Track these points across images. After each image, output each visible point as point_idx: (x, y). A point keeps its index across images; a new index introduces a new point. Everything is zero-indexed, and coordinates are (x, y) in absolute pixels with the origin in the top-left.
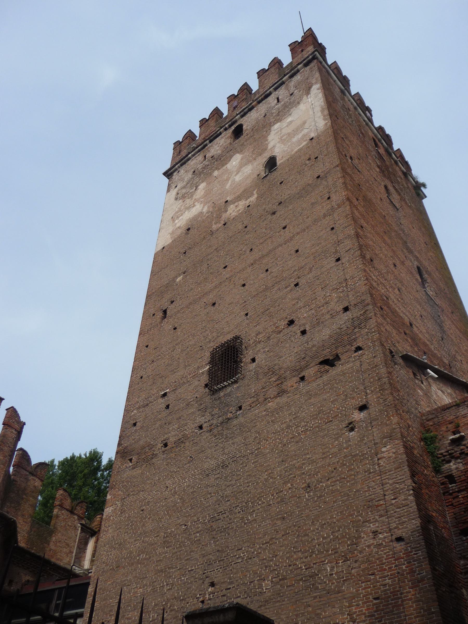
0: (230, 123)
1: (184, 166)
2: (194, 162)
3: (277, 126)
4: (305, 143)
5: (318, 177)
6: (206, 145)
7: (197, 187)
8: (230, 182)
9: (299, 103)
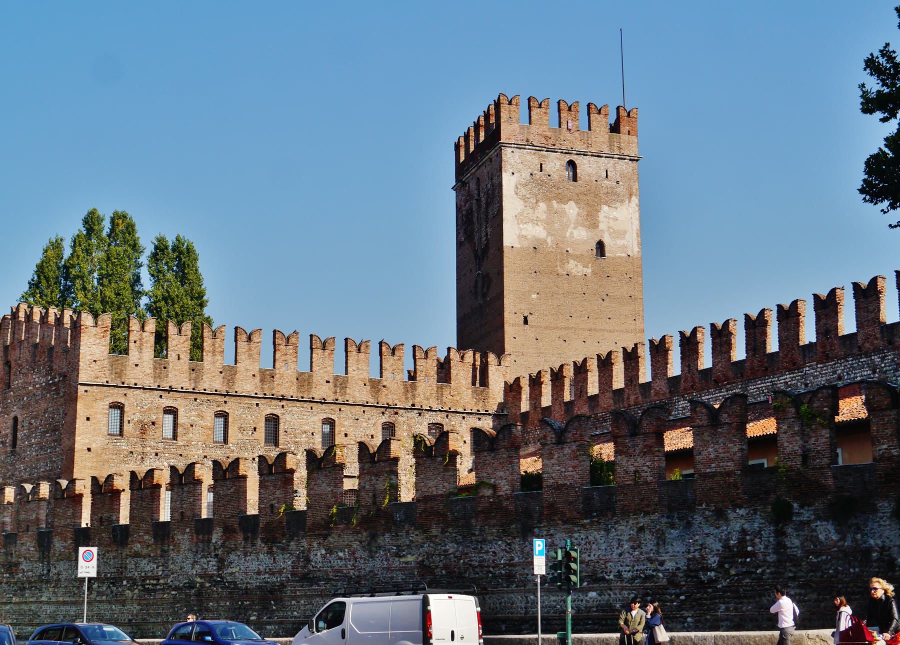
0: (567, 151)
2: (528, 158)
3: (605, 208)
4: (624, 255)
5: (631, 296)
6: (542, 151)
8: (569, 231)
9: (622, 201)
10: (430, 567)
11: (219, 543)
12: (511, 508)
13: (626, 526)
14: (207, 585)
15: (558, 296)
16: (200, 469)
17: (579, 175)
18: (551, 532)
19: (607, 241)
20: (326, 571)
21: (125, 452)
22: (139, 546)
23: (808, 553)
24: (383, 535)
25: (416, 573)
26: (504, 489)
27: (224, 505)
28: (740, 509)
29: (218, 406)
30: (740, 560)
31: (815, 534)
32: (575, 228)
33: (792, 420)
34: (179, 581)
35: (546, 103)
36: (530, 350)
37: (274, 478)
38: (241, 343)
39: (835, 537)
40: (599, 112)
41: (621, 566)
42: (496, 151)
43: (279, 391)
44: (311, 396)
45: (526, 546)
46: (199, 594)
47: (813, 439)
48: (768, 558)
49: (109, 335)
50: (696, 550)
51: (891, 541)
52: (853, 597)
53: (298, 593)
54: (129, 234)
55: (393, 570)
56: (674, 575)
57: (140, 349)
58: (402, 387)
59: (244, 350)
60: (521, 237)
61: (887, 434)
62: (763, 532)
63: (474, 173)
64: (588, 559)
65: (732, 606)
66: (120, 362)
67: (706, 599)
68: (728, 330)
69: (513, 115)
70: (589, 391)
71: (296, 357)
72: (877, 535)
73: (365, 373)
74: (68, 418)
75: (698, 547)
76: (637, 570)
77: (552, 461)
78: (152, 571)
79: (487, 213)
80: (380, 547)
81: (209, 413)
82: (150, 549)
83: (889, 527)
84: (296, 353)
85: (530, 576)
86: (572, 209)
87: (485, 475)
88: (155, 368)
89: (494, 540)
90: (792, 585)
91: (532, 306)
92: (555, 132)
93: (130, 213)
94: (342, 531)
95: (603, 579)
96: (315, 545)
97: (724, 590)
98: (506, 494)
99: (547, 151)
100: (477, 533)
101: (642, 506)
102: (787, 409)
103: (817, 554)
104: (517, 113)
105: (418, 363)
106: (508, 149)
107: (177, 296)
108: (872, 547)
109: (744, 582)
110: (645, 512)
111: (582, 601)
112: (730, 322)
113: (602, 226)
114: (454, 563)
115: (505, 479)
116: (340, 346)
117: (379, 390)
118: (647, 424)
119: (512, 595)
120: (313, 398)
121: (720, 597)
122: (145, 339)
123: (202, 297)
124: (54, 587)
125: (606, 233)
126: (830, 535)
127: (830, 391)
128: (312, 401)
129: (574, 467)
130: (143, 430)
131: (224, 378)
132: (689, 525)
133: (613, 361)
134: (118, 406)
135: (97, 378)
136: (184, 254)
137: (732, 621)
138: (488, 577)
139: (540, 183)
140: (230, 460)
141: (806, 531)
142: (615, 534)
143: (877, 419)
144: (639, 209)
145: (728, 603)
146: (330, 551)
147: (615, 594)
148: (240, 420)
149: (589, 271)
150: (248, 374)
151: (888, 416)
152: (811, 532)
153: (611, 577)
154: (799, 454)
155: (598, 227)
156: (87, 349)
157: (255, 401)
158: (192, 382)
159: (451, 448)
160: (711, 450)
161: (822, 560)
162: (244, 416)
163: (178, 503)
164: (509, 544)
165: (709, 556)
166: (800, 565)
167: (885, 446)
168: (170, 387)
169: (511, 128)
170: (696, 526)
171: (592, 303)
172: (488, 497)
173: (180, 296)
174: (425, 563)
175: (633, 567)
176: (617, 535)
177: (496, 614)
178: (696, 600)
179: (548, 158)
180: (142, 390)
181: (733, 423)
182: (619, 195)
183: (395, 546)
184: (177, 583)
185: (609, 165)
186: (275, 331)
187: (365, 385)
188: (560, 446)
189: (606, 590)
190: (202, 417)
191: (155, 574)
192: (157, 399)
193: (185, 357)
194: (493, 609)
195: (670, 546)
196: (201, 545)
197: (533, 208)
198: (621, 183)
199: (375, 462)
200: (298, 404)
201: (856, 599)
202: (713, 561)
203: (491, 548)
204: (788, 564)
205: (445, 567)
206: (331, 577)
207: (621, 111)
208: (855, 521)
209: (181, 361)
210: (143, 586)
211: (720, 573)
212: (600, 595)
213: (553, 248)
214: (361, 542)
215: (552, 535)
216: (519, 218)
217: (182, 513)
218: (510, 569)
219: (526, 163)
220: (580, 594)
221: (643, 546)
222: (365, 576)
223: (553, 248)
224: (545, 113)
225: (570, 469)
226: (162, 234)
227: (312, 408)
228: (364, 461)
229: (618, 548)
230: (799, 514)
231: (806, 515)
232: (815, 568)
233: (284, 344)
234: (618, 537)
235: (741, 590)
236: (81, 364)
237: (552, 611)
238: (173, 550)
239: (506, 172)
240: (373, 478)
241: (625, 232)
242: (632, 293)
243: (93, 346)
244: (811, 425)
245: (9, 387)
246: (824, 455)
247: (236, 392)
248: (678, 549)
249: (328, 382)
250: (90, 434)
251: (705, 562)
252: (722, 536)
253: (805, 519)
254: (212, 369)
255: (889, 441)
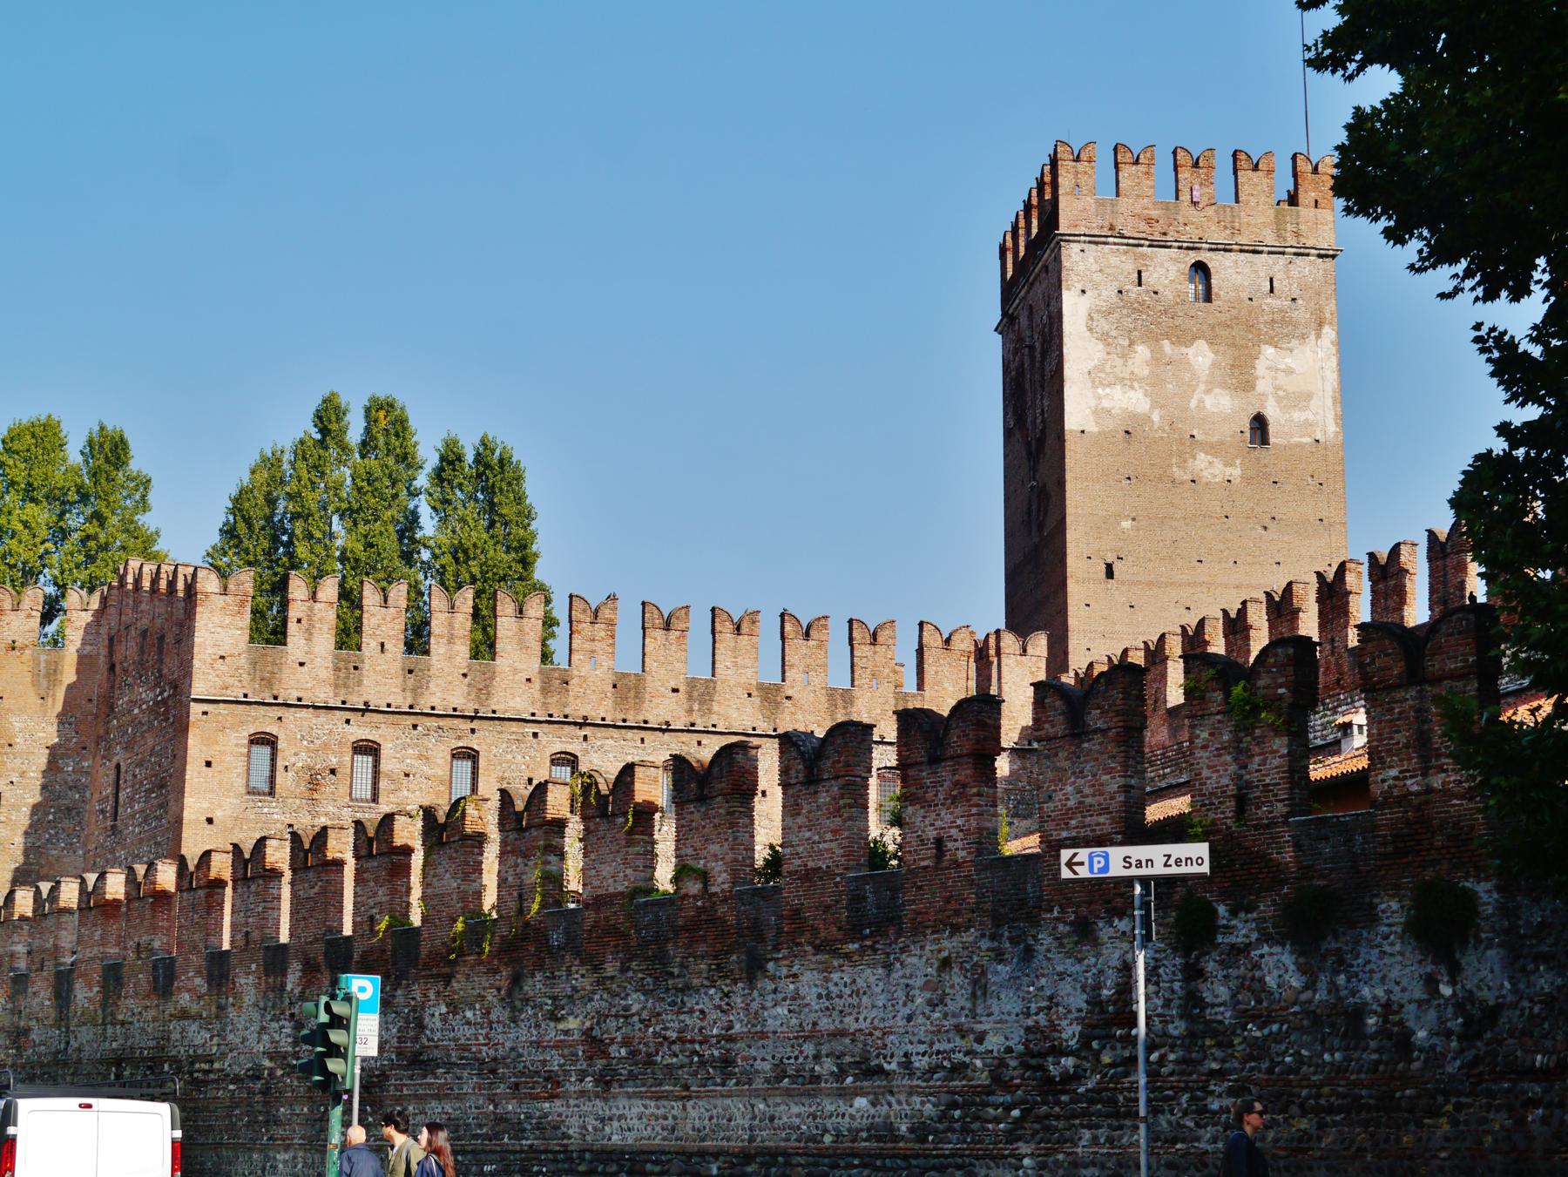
1: (1093, 246)
2: (1114, 260)
3: (1269, 351)
4: (1307, 440)
6: (1142, 246)
7: (1132, 343)
9: (1303, 337)
10: (602, 1041)
11: (296, 991)
12: (731, 919)
13: (921, 956)
14: (279, 1072)
15: (1175, 524)
16: (276, 849)
17: (1215, 290)
18: (795, 969)
19: (1271, 413)
20: (446, 1048)
21: (278, 825)
22: (187, 996)
23: (1245, 1016)
24: (533, 976)
25: (580, 1053)
26: (720, 880)
27: (304, 919)
28: (1120, 920)
29: (459, 738)
30: (1118, 1033)
31: (1258, 974)
32: (1208, 391)
33: (1219, 717)
34: (240, 1065)
35: (1148, 155)
36: (1118, 627)
37: (375, 864)
38: (504, 619)
39: (1296, 982)
40: (1256, 168)
41: (911, 1043)
42: (1052, 251)
43: (577, 710)
44: (641, 718)
45: (754, 1000)
46: (266, 1092)
47: (1257, 759)
48: (1170, 1026)
49: (248, 609)
50: (1040, 1009)
51: (1404, 990)
52: (1328, 1119)
53: (405, 1092)
54: (397, 435)
55: (545, 1047)
56: (1002, 1063)
57: (309, 634)
58: (823, 699)
59: (510, 634)
60: (1099, 412)
61: (1398, 743)
62: (1161, 971)
63: (1024, 298)
64: (854, 1026)
65: (1102, 1133)
66: (269, 659)
67: (1058, 1118)
68: (1399, 563)
69: (1083, 180)
70: (1168, 698)
71: (613, 645)
72: (1377, 976)
73: (749, 673)
74: (178, 764)
75: (1045, 1004)
76: (938, 1052)
77: (800, 820)
78: (203, 1045)
79: (1043, 369)
80: (528, 1000)
81: (441, 754)
82: (202, 1003)
83: (1399, 958)
84: (613, 637)
85: (758, 1062)
86: (1201, 356)
87: (690, 851)
88: (336, 669)
89: (703, 985)
90: (1218, 1089)
91: (1121, 544)
92: (1167, 209)
93: (402, 398)
94: (472, 967)
95: (880, 1071)
96: (432, 995)
97: (1093, 1097)
98: (722, 890)
99: (1150, 246)
100: (676, 971)
101: (947, 913)
102: (1208, 695)
103: (1263, 1020)
104: (1090, 176)
105: (856, 653)
106: (1072, 245)
107: (475, 545)
108: (1366, 1004)
109: (1125, 1080)
110: (952, 925)
111: (843, 1115)
112: (1402, 547)
113: (1262, 386)
114: (639, 1034)
115: (722, 859)
116: (700, 622)
117: (777, 704)
118: (959, 737)
119: (728, 1101)
120: (646, 722)
121: (1085, 1114)
122: (319, 616)
123: (525, 547)
124: (73, 1074)
125: (1270, 397)
126: (1287, 977)
127: (1291, 651)
128: (644, 727)
129: (835, 832)
130: (314, 784)
131: (469, 685)
132: (1028, 954)
133: (1207, 637)
134: (265, 740)
135: (227, 688)
136: (492, 469)
137: (1103, 1167)
138: (691, 1063)
139: (1138, 308)
140: (317, 829)
141: (1242, 968)
142: (900, 973)
143: (1379, 709)
144: (1338, 351)
145: (1098, 1127)
146: (454, 1008)
147: (899, 1103)
148: (500, 764)
149: (1236, 472)
150: (517, 677)
151: (1401, 702)
152: (1251, 970)
153: (894, 1066)
154: (1229, 793)
155: (1253, 387)
156: (207, 635)
157: (531, 729)
158: (408, 694)
159: (639, 798)
160: (1069, 789)
161: (1271, 1033)
162: (509, 757)
163: (242, 914)
164: (727, 995)
165: (1064, 1023)
166: (1231, 1045)
167: (1394, 772)
168: (366, 704)
169: (1080, 205)
170: (1041, 957)
171: (1243, 533)
172: (695, 897)
173: (479, 545)
174: (594, 1033)
175: (932, 1044)
176: (904, 976)
177: (703, 1140)
178: (1039, 1119)
179: (1152, 259)
180: (311, 710)
181: (1109, 729)
182: (1296, 326)
183: (550, 998)
184: (236, 1069)
185: (1276, 268)
186: (851, 622)
187: (749, 695)
188: (812, 789)
189: (883, 1094)
190: (427, 758)
191: (208, 1052)
192: (341, 726)
193: (396, 648)
194: (699, 1131)
195: (995, 1001)
196: (271, 995)
197: (1124, 357)
198: (1300, 302)
199: (521, 830)
200: (614, 733)
201: (1335, 1124)
202: (1070, 1032)
203: (697, 1004)
204: (1208, 1042)
205: (626, 1042)
206: (453, 1060)
207: (1299, 162)
208: (1333, 945)
209: (388, 655)
210: (191, 1073)
211: (1085, 1058)
212: (874, 1104)
213: (1164, 431)
214: (499, 990)
215: (795, 976)
216: (1096, 377)
217: (247, 933)
218: (728, 1046)
219: (1109, 271)
220: (841, 1103)
221: (949, 1002)
222: (504, 1058)
223: (1164, 431)
224: (1147, 173)
225: (829, 836)
226: (453, 435)
227: (642, 740)
228: (507, 827)
229: (905, 1005)
230: (1228, 929)
231: (1243, 931)
232: (1258, 1050)
233: (588, 619)
234: (906, 981)
235: (1121, 1098)
236: (196, 662)
237: (795, 1137)
238: (233, 1005)
239: (1069, 289)
240: (519, 861)
241: (1309, 396)
242: (1323, 515)
243: (219, 629)
244: (1254, 728)
245: (112, 708)
246: (1276, 795)
247: (494, 712)
248: (1008, 1007)
249: (675, 690)
250: (212, 791)
251: (1056, 1035)
252: (1087, 979)
253: (1239, 940)
254: (446, 670)
255: (1401, 760)
